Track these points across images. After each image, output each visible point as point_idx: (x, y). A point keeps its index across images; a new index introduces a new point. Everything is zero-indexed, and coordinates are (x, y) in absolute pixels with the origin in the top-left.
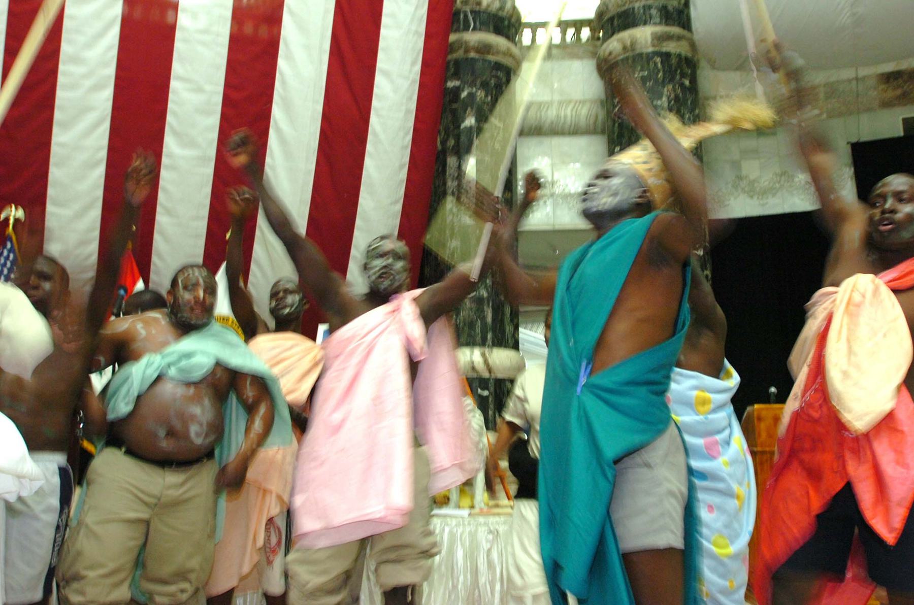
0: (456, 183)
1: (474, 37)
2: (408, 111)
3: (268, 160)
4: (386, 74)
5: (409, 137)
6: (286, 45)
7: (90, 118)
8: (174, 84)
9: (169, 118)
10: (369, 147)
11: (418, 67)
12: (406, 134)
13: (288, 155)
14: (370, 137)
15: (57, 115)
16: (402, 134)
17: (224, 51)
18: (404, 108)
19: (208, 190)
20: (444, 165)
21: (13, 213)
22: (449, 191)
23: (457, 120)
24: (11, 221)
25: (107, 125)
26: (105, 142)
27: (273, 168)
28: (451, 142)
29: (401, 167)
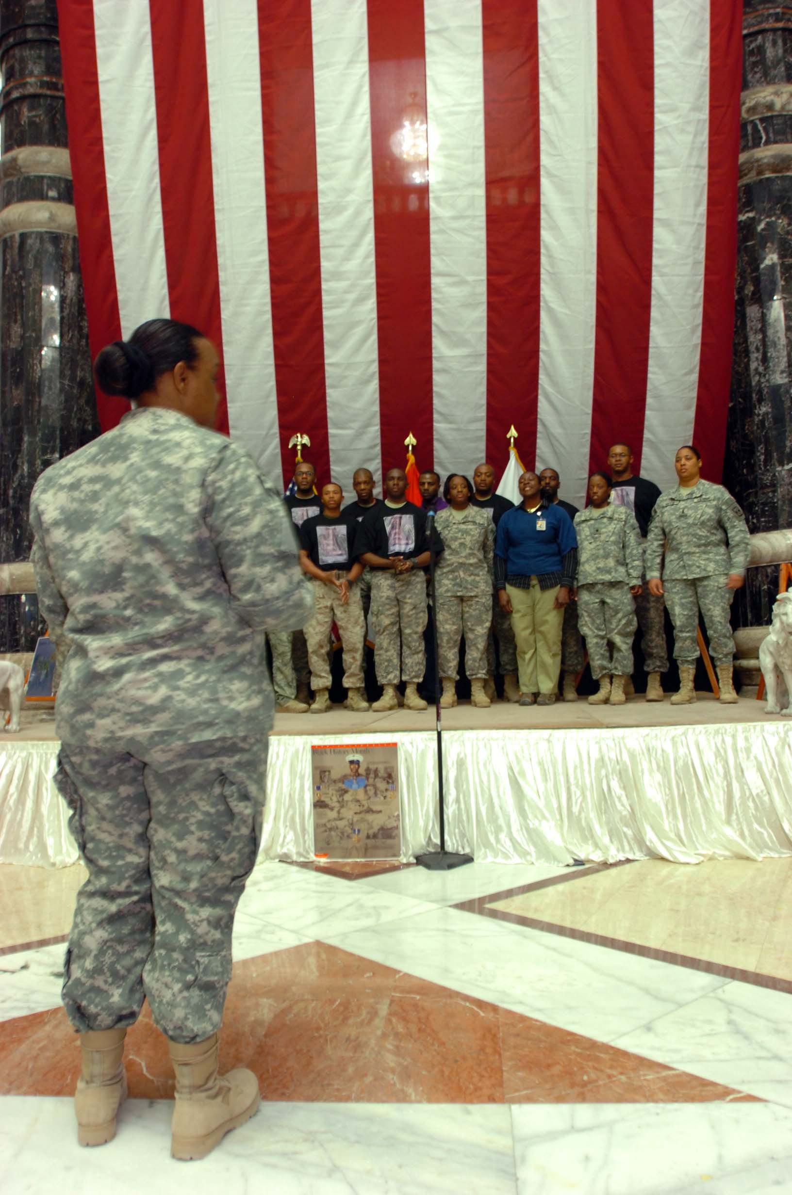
0: (760, 336)
1: (766, 153)
2: (696, 263)
3: (542, 346)
4: (666, 223)
5: (701, 293)
6: (547, 212)
7: (358, 332)
8: (435, 281)
9: (435, 319)
10: (654, 313)
11: (703, 208)
12: (696, 291)
13: (564, 337)
14: (654, 302)
15: (327, 335)
16: (690, 291)
17: (482, 234)
18: (690, 261)
19: (483, 388)
20: (743, 317)
21: (299, 439)
22: (752, 348)
23: (755, 261)
24: (299, 447)
25: (374, 337)
26: (375, 355)
27: (549, 354)
28: (750, 289)
29: (693, 331)
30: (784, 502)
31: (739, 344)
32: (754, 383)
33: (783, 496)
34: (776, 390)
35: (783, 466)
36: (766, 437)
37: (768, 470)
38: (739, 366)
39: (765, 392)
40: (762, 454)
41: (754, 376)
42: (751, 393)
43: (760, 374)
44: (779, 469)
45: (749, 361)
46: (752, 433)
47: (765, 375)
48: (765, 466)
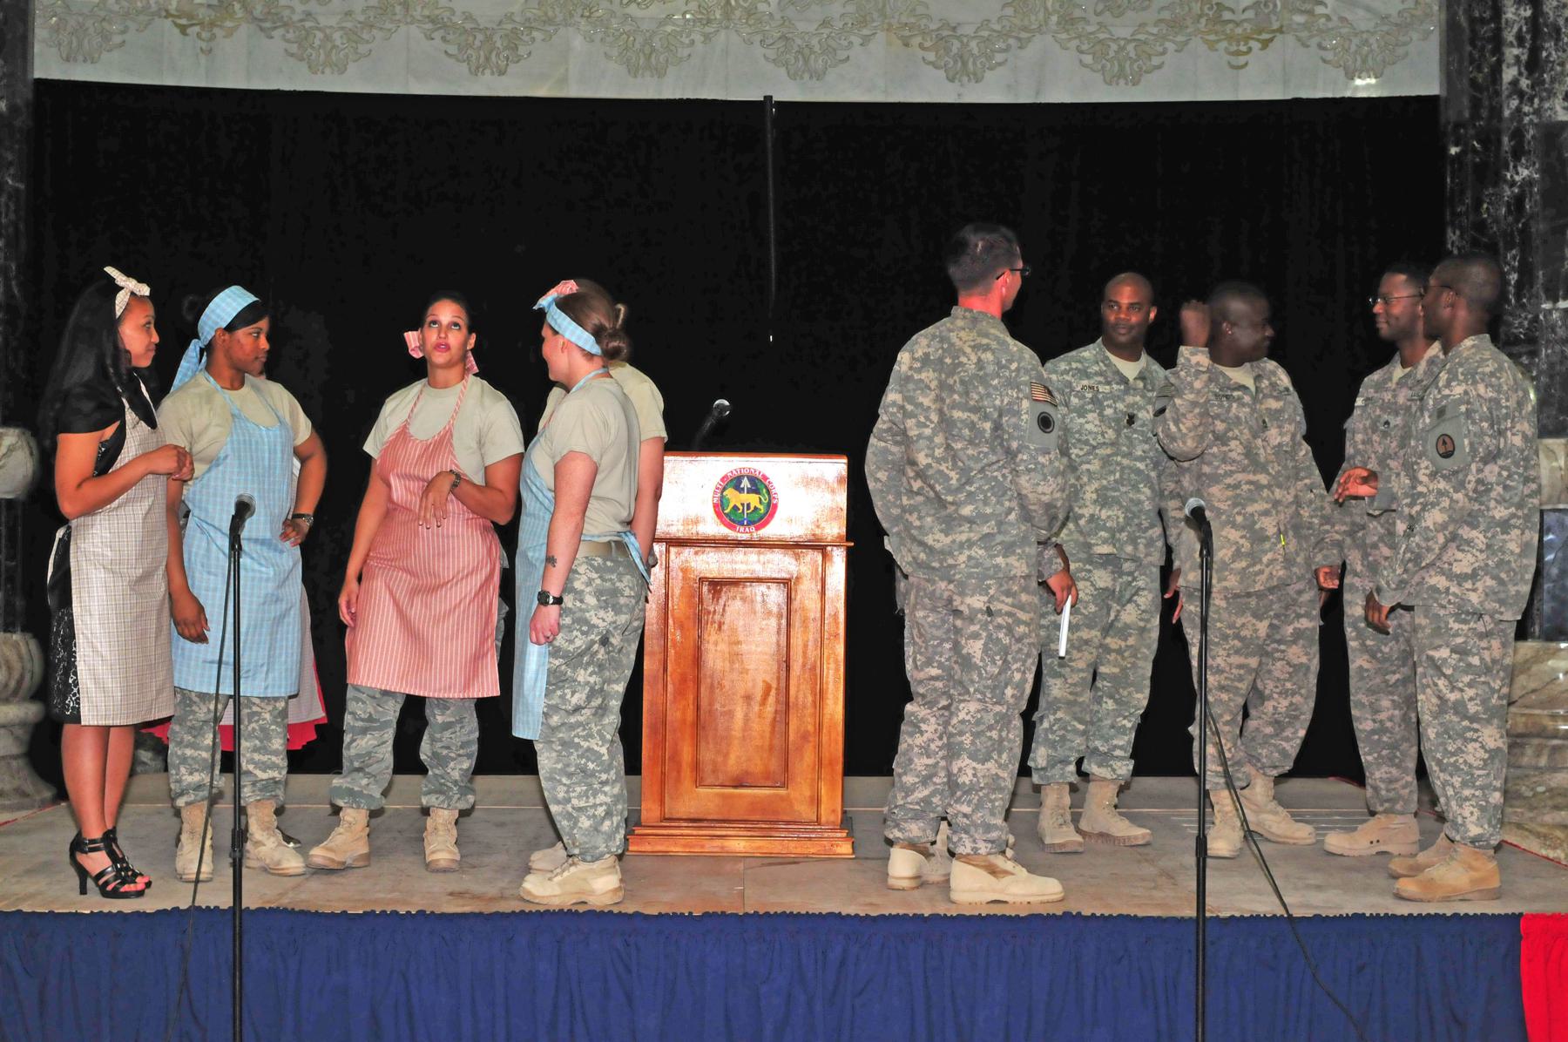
22: (1509, 36)
30: (1551, 377)
31: (1483, 21)
32: (1507, 113)
33: (1551, 365)
34: (1552, 133)
35: (1556, 301)
36: (1524, 232)
37: (1523, 306)
38: (1479, 69)
39: (1529, 137)
40: (1513, 269)
41: (1509, 96)
42: (1499, 133)
43: (1521, 95)
44: (1546, 306)
45: (1500, 62)
46: (1496, 221)
47: (1531, 100)
48: (1518, 296)
